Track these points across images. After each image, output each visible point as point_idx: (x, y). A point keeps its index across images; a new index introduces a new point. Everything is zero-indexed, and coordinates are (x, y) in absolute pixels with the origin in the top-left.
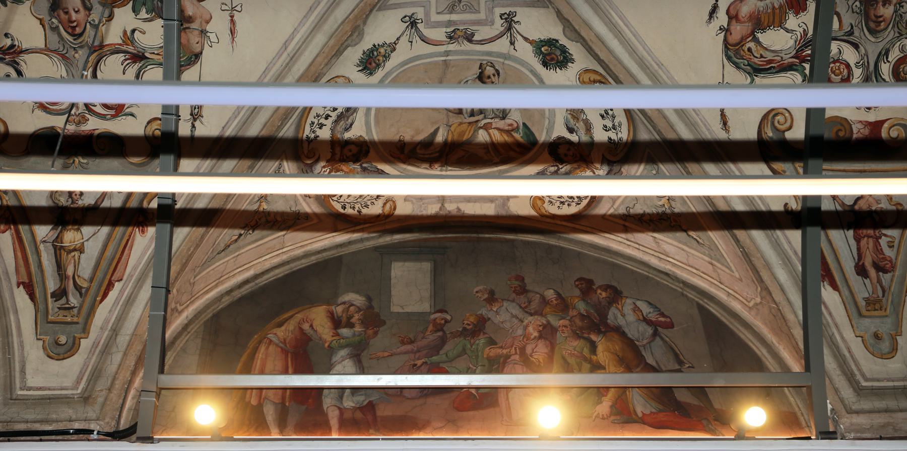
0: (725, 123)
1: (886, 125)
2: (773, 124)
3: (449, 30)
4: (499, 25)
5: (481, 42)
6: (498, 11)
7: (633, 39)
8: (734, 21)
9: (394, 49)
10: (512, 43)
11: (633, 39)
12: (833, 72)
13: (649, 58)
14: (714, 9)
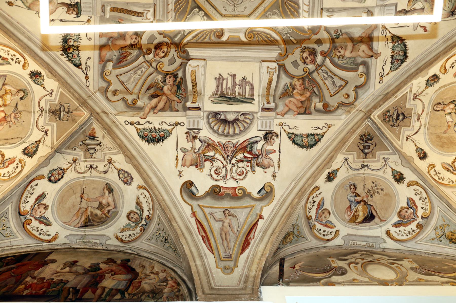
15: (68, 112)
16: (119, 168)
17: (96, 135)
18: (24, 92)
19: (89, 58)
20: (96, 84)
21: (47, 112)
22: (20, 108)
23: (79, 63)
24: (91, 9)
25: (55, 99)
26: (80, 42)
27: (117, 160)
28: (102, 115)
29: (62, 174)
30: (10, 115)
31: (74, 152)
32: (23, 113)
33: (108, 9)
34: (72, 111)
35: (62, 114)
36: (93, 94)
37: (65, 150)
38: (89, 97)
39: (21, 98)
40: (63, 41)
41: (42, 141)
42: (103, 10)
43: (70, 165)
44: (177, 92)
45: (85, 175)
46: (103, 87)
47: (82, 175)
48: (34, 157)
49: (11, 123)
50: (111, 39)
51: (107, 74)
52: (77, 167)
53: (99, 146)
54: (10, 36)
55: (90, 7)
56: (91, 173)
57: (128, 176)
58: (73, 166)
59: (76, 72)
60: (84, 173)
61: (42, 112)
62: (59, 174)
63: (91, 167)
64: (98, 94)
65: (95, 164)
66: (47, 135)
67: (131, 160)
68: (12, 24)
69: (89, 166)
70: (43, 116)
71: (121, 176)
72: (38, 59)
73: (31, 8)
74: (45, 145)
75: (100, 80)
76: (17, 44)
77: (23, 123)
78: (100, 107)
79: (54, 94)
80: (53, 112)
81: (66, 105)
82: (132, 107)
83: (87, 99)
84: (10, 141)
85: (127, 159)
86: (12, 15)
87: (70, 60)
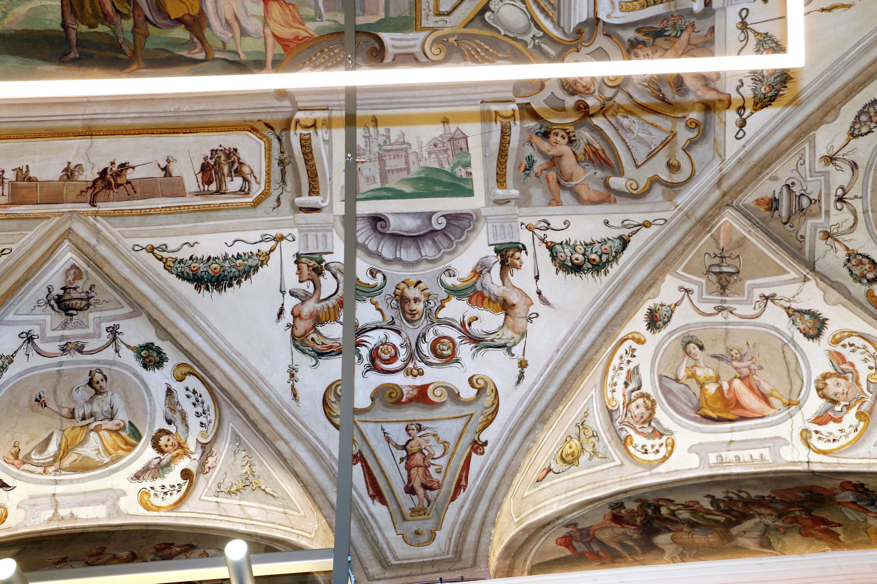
0: (295, 395)
1: (431, 387)
2: (335, 392)
3: (62, 343)
4: (105, 337)
5: (90, 353)
6: (105, 325)
7: (215, 336)
8: (298, 319)
9: (12, 361)
10: (117, 351)
11: (215, 336)
12: (383, 352)
13: (230, 351)
14: (281, 312)
15: (722, 258)
16: (847, 136)
17: (770, 195)
18: (689, 343)
19: (607, 223)
20: (659, 207)
21: (724, 298)
22: (720, 350)
23: (618, 241)
24: (506, 225)
25: (697, 282)
26: (576, 241)
27: (828, 141)
28: (725, 186)
29: (860, 257)
30: (736, 368)
31: (807, 239)
32: (730, 344)
33: (500, 193)
34: (718, 248)
35: (725, 269)
36: (680, 210)
37: (807, 255)
38: (687, 216)
39: (701, 348)
40: (579, 272)
41: (787, 305)
42: (506, 202)
43: (837, 244)
44: (669, 36)
45: (859, 210)
46: (663, 192)
47: (860, 216)
48: (824, 315)
49: (753, 367)
50: (563, 182)
51: (634, 186)
52: (840, 230)
53: (794, 189)
54: (591, 360)
55: (502, 226)
56: (856, 197)
57: (868, 113)
58: (840, 238)
59: (639, 245)
60: (854, 213)
61: (724, 309)
62: (861, 262)
63: (840, 200)
64: (681, 200)
65: (833, 192)
66: (774, 296)
67: (834, 107)
68: (564, 360)
69: (839, 205)
70: (733, 306)
71: (864, 130)
72: (625, 312)
73: (522, 330)
74: (796, 298)
75: (649, 198)
76: (603, 349)
77: (751, 344)
78: (709, 193)
79: (687, 286)
80: (724, 288)
81: (709, 261)
82: (704, 129)
83: (693, 219)
84: (793, 367)
85: (828, 119)
86: (546, 361)
87: (615, 258)
